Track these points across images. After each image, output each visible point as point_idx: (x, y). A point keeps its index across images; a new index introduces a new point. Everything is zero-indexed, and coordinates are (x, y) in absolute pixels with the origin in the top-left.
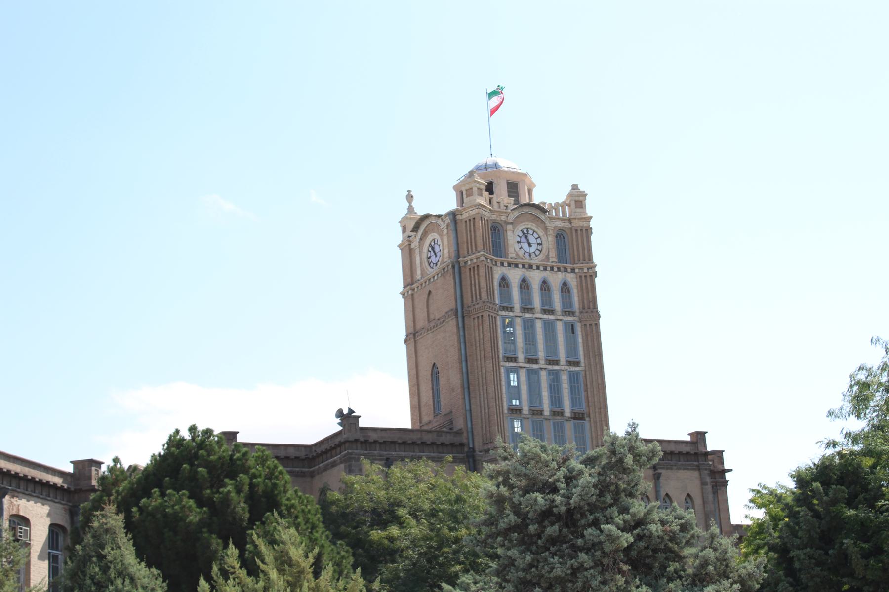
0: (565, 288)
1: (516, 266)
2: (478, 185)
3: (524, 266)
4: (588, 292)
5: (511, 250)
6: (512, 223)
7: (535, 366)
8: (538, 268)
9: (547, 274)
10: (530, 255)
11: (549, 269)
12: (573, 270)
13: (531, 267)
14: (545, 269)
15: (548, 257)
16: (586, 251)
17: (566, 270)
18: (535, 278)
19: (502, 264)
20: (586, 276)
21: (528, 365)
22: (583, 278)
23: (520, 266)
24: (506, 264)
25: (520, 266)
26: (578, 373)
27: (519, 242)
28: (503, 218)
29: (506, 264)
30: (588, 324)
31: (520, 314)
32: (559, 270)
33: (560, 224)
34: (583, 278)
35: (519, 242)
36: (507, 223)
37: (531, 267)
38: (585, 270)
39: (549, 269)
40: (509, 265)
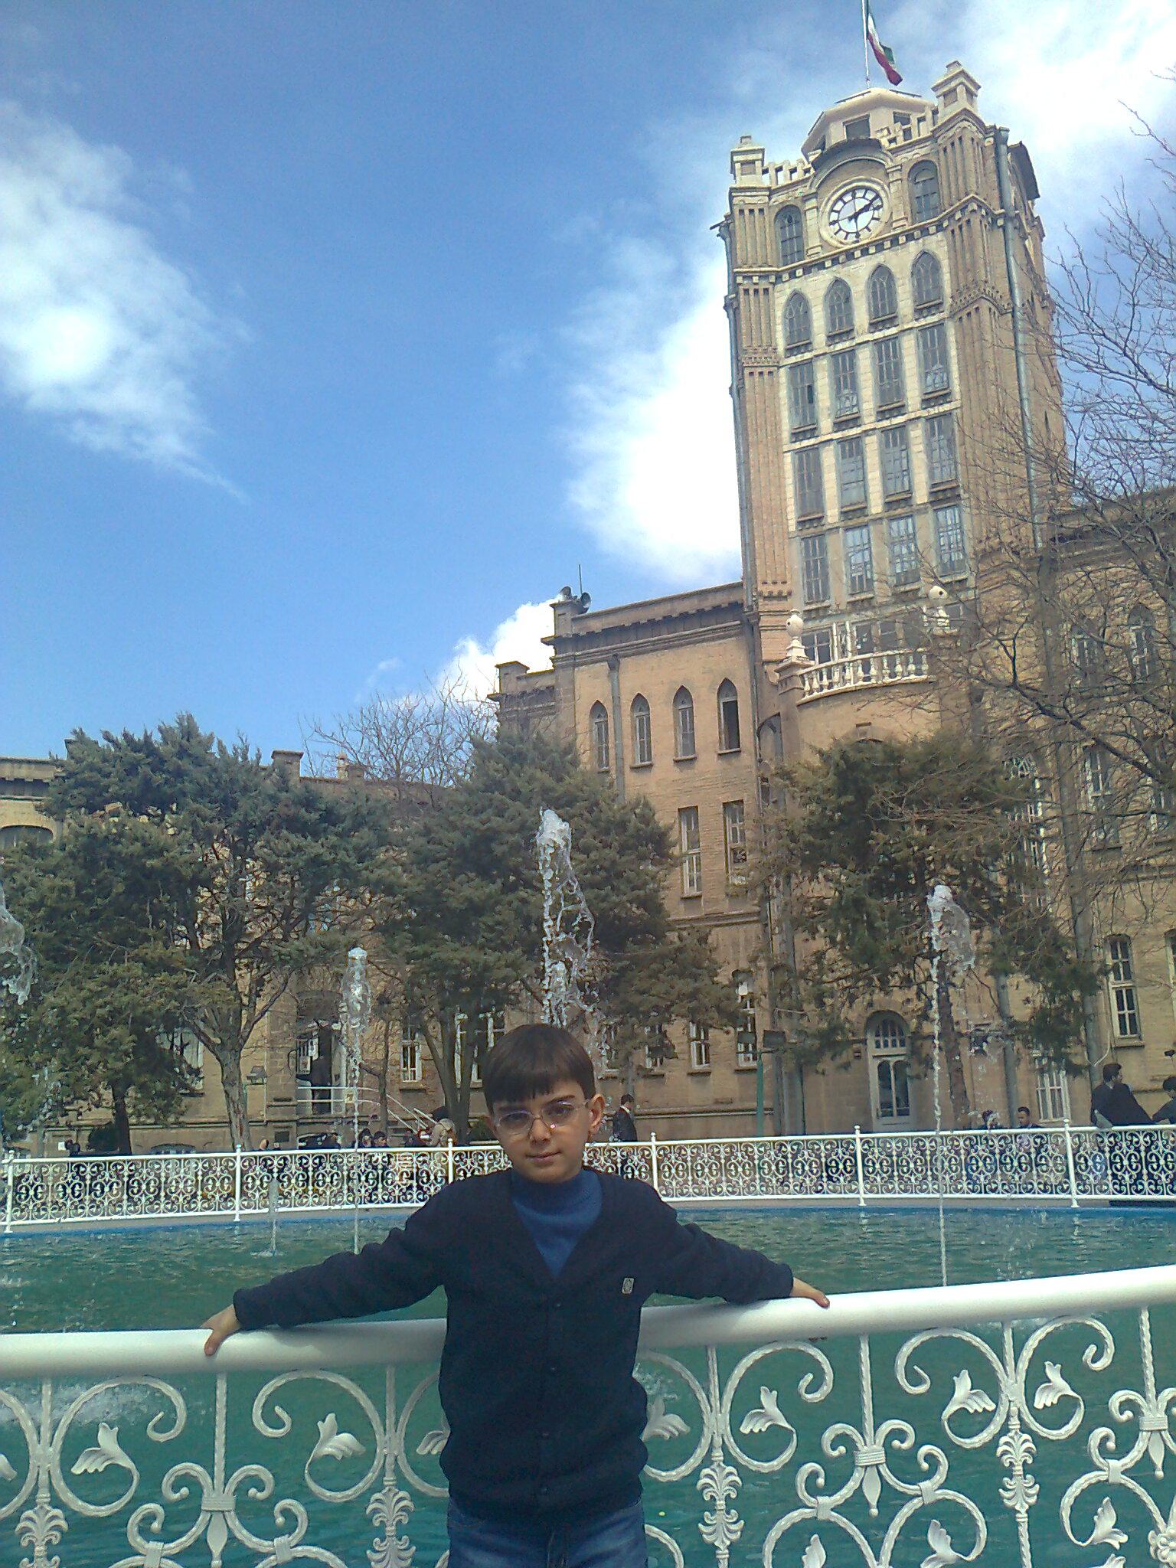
0: (926, 265)
1: (820, 265)
2: (741, 158)
3: (835, 261)
4: (964, 257)
5: (813, 241)
6: (815, 195)
7: (854, 432)
8: (865, 251)
9: (880, 258)
10: (858, 235)
11: (887, 244)
12: (940, 228)
13: (850, 255)
14: (879, 246)
15: (889, 224)
16: (961, 178)
17: (924, 231)
18: (858, 274)
19: (793, 275)
20: (960, 227)
21: (839, 435)
22: (957, 231)
23: (828, 264)
24: (799, 272)
25: (828, 264)
26: (948, 414)
27: (833, 223)
28: (800, 191)
29: (799, 272)
30: (964, 314)
31: (827, 350)
32: (910, 237)
33: (918, 153)
34: (957, 231)
35: (833, 223)
36: (806, 198)
37: (850, 255)
38: (958, 216)
39: (887, 244)
40: (807, 269)
